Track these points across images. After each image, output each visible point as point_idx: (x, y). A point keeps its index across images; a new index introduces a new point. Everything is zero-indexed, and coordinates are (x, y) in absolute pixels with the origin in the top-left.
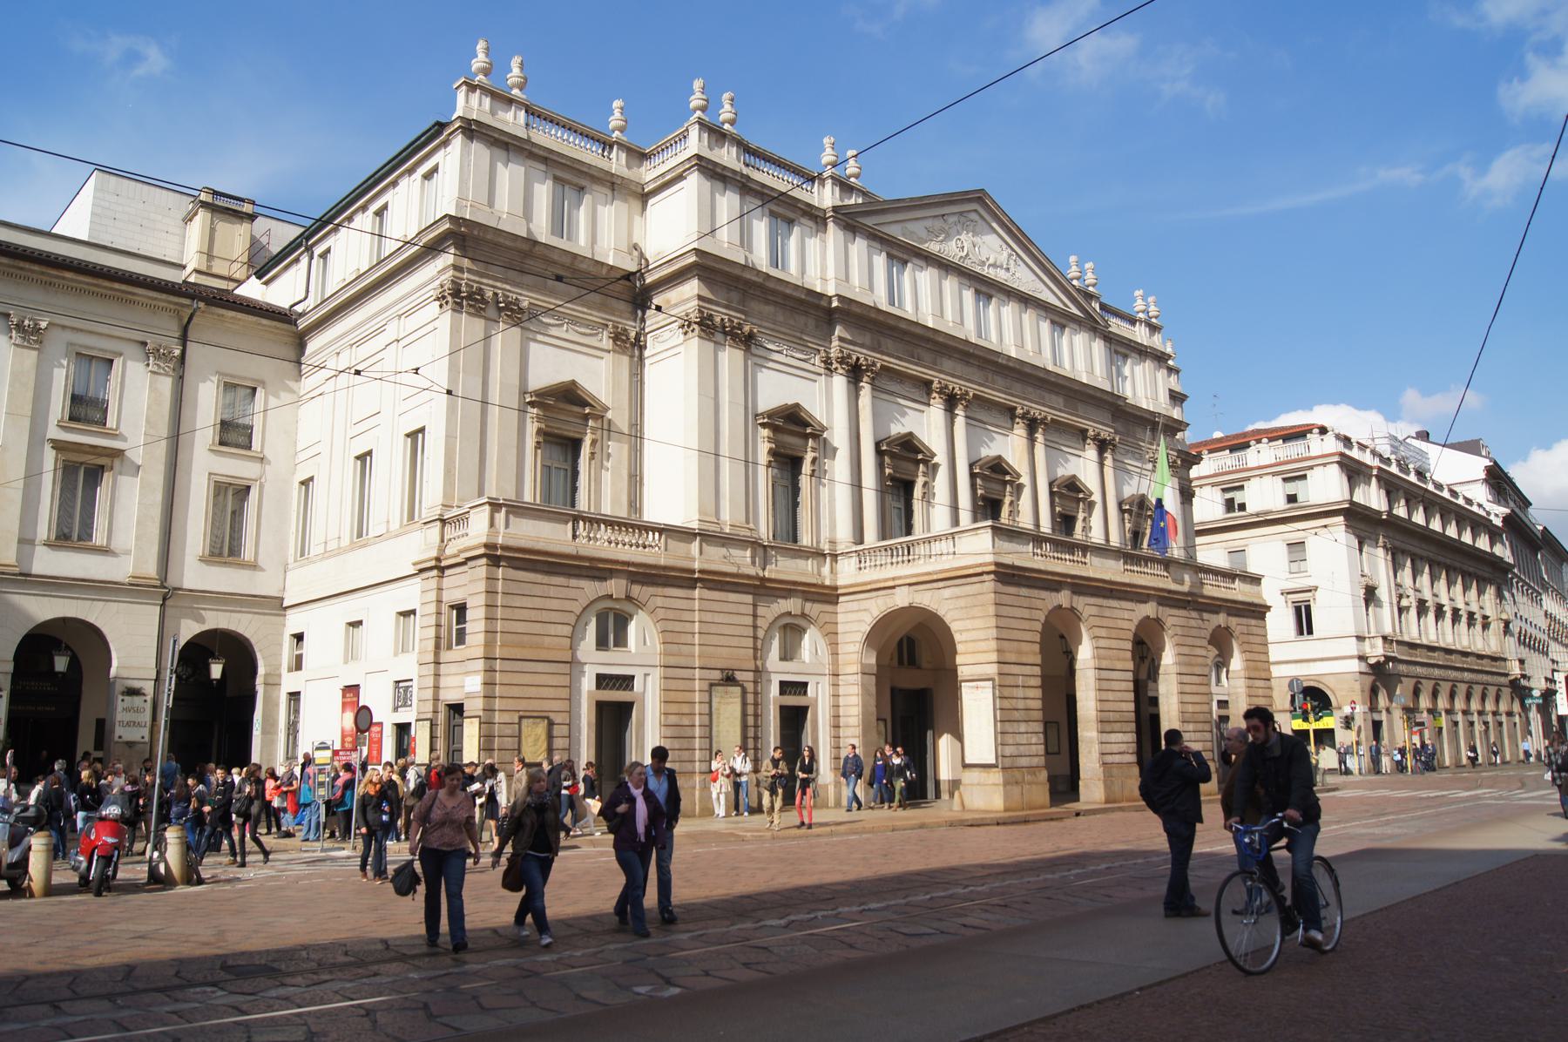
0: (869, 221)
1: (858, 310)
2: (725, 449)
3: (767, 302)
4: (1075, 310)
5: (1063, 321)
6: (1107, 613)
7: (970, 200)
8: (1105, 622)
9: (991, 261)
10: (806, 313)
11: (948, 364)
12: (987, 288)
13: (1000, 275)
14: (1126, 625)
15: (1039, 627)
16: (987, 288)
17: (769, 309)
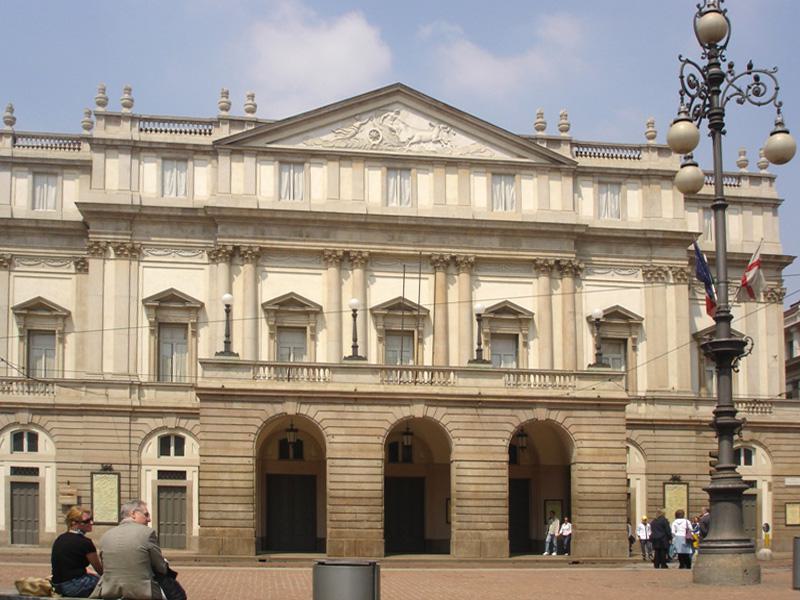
0: (261, 143)
1: (230, 214)
2: (109, 324)
3: (154, 223)
4: (531, 160)
5: (512, 171)
6: (350, 416)
7: (388, 95)
8: (345, 423)
9: (414, 140)
10: (193, 224)
11: (342, 235)
12: (399, 164)
13: (429, 149)
14: (379, 424)
15: (254, 430)
16: (399, 164)
17: (160, 227)
